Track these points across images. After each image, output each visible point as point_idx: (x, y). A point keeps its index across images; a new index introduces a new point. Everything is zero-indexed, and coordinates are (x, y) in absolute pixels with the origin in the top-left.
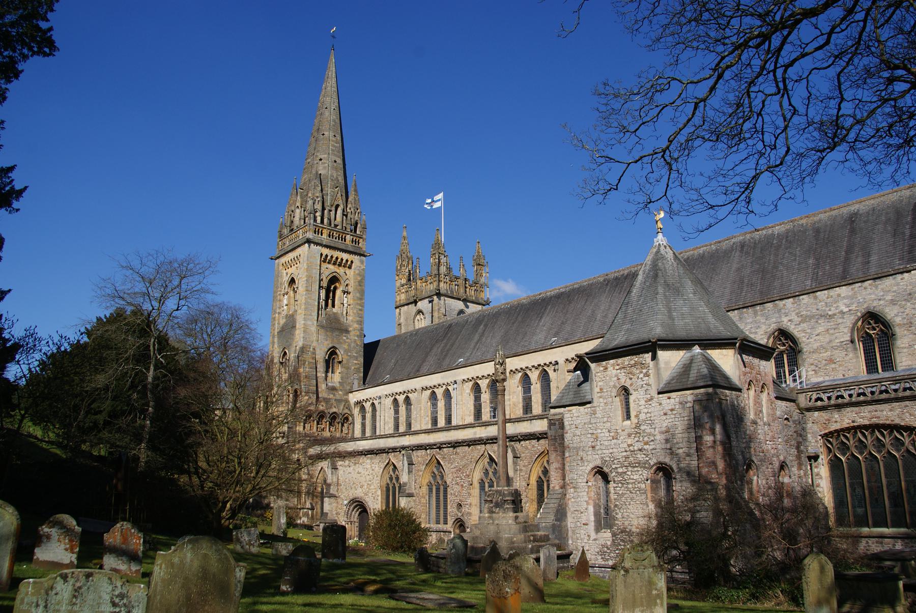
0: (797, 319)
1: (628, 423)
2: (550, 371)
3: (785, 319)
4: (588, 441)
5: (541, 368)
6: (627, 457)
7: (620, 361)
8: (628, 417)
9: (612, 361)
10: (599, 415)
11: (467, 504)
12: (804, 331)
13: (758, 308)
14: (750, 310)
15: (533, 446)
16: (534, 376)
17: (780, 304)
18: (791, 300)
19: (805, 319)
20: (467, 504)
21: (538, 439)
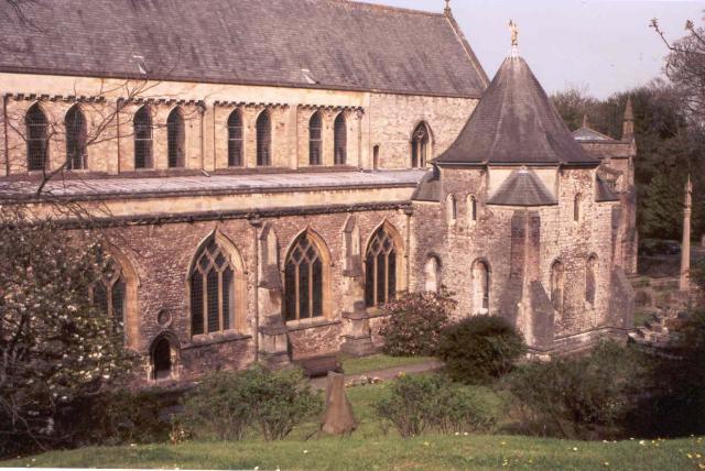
0: (434, 116)
1: (575, 223)
2: (187, 112)
3: (427, 113)
4: (553, 237)
5: (174, 106)
6: (575, 250)
7: (577, 171)
8: (576, 218)
9: (572, 171)
10: (561, 215)
11: (180, 309)
12: (437, 127)
13: (410, 98)
14: (404, 98)
15: (290, 224)
16: (161, 115)
17: (426, 99)
18: (431, 98)
19: (439, 117)
20: (180, 309)
21: (328, 213)
